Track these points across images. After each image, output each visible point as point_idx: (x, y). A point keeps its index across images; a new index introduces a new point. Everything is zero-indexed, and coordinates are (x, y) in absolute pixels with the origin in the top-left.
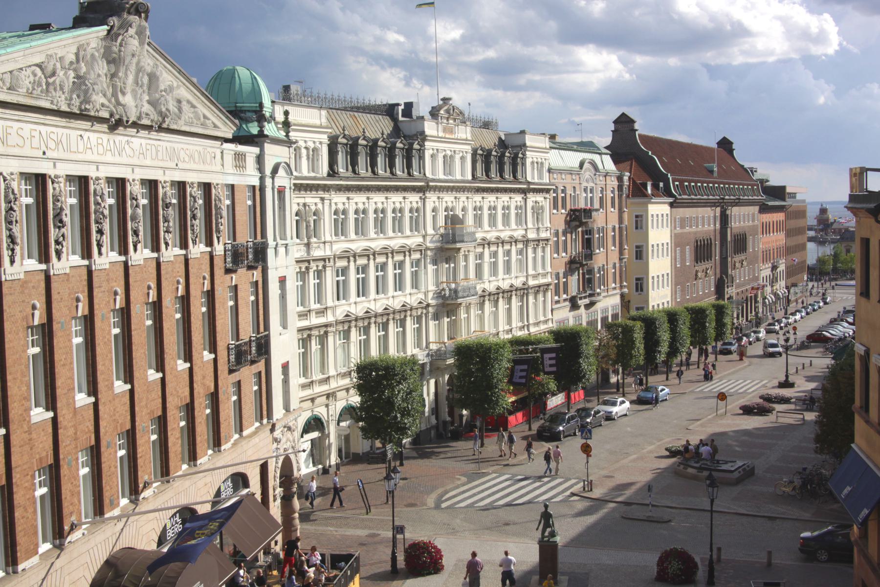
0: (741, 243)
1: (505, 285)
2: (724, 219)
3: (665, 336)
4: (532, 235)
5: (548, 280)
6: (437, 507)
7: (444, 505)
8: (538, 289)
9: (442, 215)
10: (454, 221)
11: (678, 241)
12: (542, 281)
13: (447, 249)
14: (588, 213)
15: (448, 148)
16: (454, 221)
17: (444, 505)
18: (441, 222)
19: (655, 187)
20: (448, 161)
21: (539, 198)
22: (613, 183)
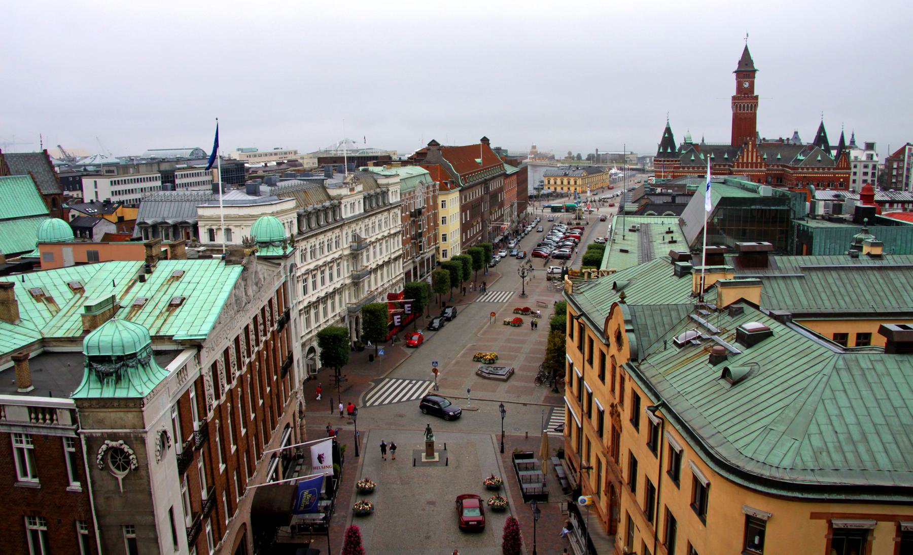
0: (494, 196)
1: (380, 263)
2: (487, 188)
3: (460, 273)
4: (392, 232)
5: (401, 252)
6: (365, 406)
7: (368, 404)
8: (396, 259)
9: (350, 235)
10: (357, 238)
11: (463, 209)
12: (397, 254)
13: (355, 255)
14: (419, 212)
15: (351, 200)
16: (357, 238)
17: (368, 404)
18: (350, 239)
19: (452, 182)
20: (352, 205)
21: (396, 210)
22: (431, 189)
